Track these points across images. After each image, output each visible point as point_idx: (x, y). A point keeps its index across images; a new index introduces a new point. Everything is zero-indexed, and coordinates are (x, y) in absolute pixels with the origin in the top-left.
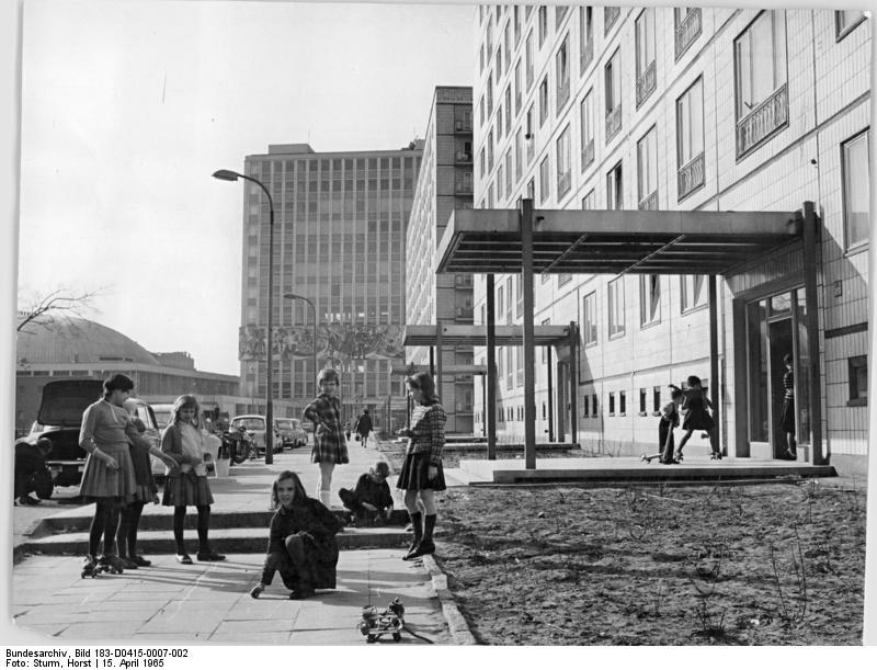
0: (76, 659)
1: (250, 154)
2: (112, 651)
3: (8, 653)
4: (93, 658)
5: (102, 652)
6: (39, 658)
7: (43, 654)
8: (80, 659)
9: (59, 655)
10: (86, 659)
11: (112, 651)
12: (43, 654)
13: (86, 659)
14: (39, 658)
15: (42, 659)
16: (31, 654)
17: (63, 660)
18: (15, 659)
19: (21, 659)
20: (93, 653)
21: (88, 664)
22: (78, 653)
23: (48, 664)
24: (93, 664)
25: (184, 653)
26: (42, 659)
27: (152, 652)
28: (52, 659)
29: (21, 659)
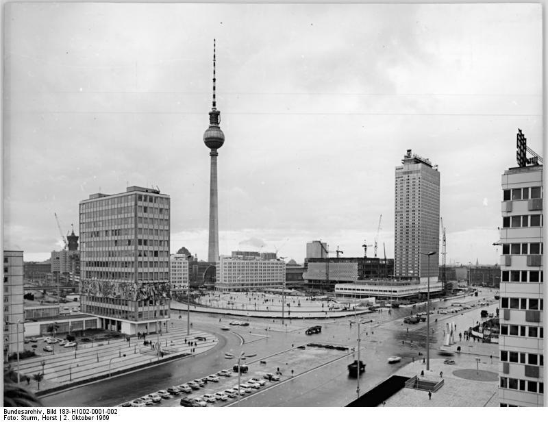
0: (48, 415)
1: (186, 248)
2: (70, 410)
3: (5, 411)
4: (58, 414)
5: (64, 411)
6: (24, 414)
7: (27, 412)
8: (50, 415)
9: (37, 412)
10: (53, 415)
11: (70, 410)
12: (27, 412)
13: (53, 415)
14: (24, 414)
15: (26, 415)
16: (19, 412)
17: (39, 416)
18: (10, 415)
19: (13, 415)
20: (58, 412)
21: (55, 418)
22: (48, 412)
23: (30, 418)
24: (58, 418)
25: (115, 411)
26: (26, 415)
27: (95, 411)
28: (33, 415)
29: (13, 415)
